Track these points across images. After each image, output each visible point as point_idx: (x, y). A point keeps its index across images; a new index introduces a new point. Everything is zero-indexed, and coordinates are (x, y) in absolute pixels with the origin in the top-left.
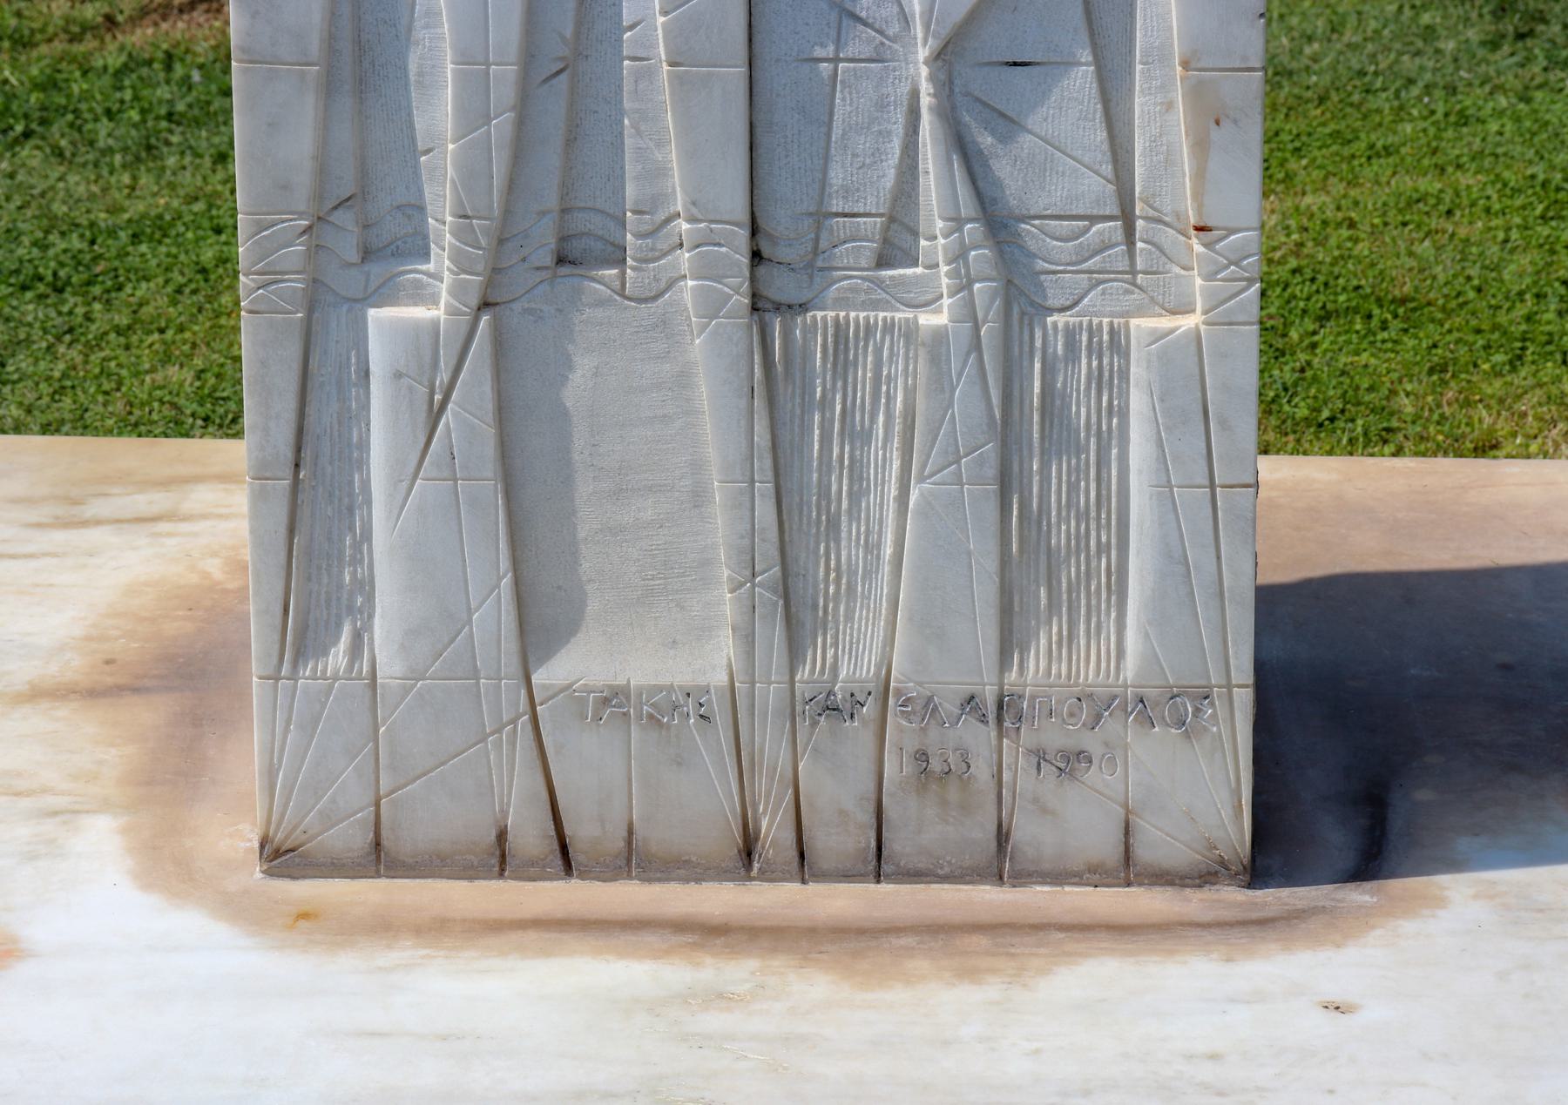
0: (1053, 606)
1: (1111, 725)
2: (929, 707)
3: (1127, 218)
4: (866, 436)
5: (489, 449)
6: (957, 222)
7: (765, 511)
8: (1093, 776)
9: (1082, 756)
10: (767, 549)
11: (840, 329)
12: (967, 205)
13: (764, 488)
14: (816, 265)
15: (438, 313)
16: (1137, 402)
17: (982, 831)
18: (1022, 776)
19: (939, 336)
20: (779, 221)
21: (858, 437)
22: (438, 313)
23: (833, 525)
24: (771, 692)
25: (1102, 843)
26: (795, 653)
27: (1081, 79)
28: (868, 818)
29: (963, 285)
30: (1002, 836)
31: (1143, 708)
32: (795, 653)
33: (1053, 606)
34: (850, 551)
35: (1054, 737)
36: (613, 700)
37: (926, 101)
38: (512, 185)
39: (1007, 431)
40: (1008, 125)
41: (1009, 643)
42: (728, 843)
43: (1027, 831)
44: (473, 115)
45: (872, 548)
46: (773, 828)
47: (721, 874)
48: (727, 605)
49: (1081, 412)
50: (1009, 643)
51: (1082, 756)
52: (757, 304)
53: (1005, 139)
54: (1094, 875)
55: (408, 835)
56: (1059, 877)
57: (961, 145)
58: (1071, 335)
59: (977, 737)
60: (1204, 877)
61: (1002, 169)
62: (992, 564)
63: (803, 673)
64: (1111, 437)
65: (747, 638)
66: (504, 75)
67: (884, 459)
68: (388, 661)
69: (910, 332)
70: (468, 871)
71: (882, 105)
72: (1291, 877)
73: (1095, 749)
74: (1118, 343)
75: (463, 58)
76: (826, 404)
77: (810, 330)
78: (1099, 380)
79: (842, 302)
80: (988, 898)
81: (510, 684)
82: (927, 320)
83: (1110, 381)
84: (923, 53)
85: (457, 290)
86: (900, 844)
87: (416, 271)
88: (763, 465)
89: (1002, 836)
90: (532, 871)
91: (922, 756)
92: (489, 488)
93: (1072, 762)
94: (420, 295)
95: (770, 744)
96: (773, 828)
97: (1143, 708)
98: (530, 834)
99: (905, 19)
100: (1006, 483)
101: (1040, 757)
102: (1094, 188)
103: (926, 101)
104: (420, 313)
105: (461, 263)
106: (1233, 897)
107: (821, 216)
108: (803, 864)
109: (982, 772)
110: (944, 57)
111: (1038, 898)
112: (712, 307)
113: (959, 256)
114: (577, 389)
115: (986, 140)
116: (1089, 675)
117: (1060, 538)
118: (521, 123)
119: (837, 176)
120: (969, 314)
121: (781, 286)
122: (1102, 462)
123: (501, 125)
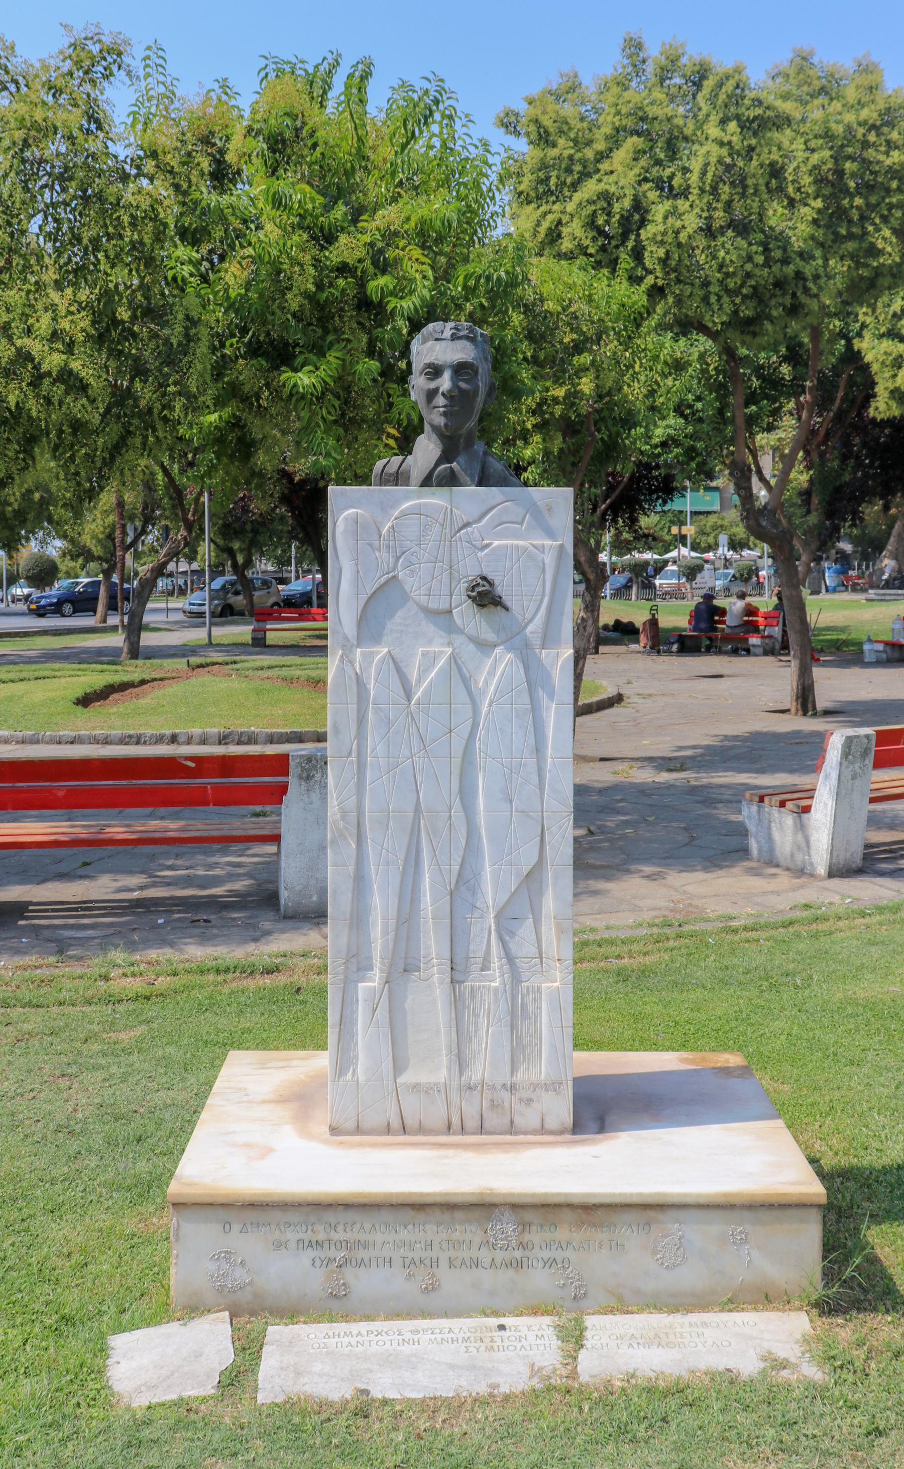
0: (524, 1060)
1: (538, 1091)
2: (493, 1088)
3: (541, 958)
4: (478, 1015)
5: (387, 1020)
6: (501, 959)
7: (454, 1035)
8: (534, 1105)
9: (531, 1100)
10: (454, 1045)
11: (472, 987)
12: (503, 955)
13: (454, 1029)
14: (466, 971)
15: (376, 984)
16: (544, 1005)
17: (507, 1121)
18: (517, 1106)
19: (496, 989)
20: (457, 960)
21: (477, 1016)
22: (376, 984)
23: (470, 1039)
24: (455, 1084)
25: (535, 1123)
26: (461, 1074)
27: (530, 922)
28: (478, 1117)
29: (502, 975)
30: (512, 1122)
31: (546, 1087)
32: (461, 1074)
33: (524, 1060)
34: (474, 1046)
35: (525, 1095)
36: (416, 1086)
37: (493, 928)
38: (393, 952)
39: (513, 1013)
40: (512, 934)
41: (513, 1070)
42: (443, 1124)
43: (518, 1120)
44: (385, 933)
45: (480, 1045)
46: (456, 1121)
47: (443, 1134)
48: (445, 1060)
49: (531, 1008)
50: (513, 1070)
51: (531, 1100)
52: (452, 981)
53: (512, 938)
54: (534, 1132)
55: (366, 1124)
56: (526, 1133)
57: (501, 939)
58: (528, 988)
59: (506, 1095)
60: (561, 1132)
61: (511, 945)
62: (509, 1049)
63: (463, 1078)
64: (537, 1015)
65: (449, 1069)
66: (393, 922)
67: (483, 1021)
68: (361, 1075)
69: (489, 988)
70: (380, 1134)
71: (482, 929)
72: (582, 1133)
73: (535, 1098)
74: (539, 990)
75: (383, 918)
76: (469, 1007)
77: (465, 988)
78: (535, 1000)
79: (472, 981)
80: (508, 1138)
81: (391, 1082)
82: (493, 984)
83: (537, 1001)
84: (492, 916)
85: (380, 978)
86: (486, 1125)
87: (369, 974)
88: (454, 1023)
89: (512, 1122)
90: (396, 1133)
91: (492, 1101)
92: (387, 1030)
93: (529, 1101)
94: (371, 980)
95: (455, 1097)
96: (456, 1121)
97: (546, 1087)
98: (396, 1124)
99: (488, 907)
100: (513, 1027)
101: (521, 1100)
102: (534, 950)
103: (493, 928)
104: (371, 984)
105: (381, 971)
106: (569, 1137)
107: (468, 958)
108: (463, 1130)
109: (507, 1104)
110: (498, 917)
111: (521, 1138)
112: (441, 982)
113: (501, 968)
114: (408, 1005)
115: (507, 938)
116: (533, 1078)
117: (525, 1042)
118: (396, 935)
119: (471, 948)
120: (503, 982)
121: (458, 976)
122: (536, 1021)
123: (392, 935)
